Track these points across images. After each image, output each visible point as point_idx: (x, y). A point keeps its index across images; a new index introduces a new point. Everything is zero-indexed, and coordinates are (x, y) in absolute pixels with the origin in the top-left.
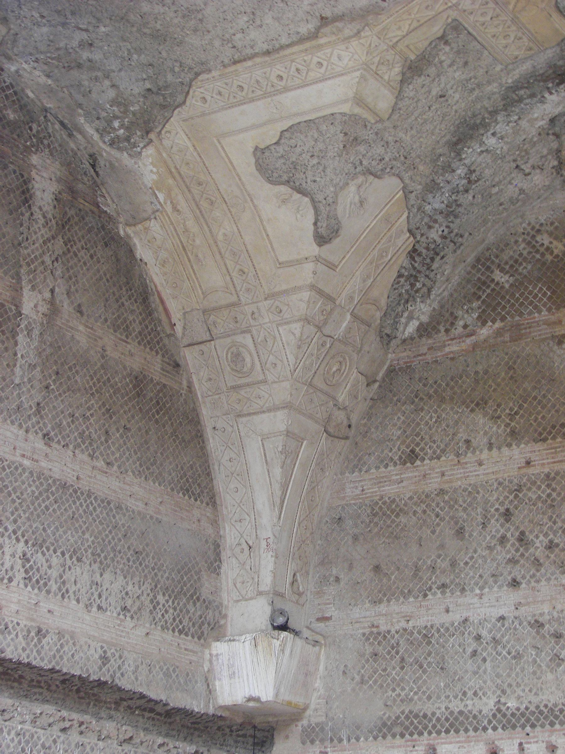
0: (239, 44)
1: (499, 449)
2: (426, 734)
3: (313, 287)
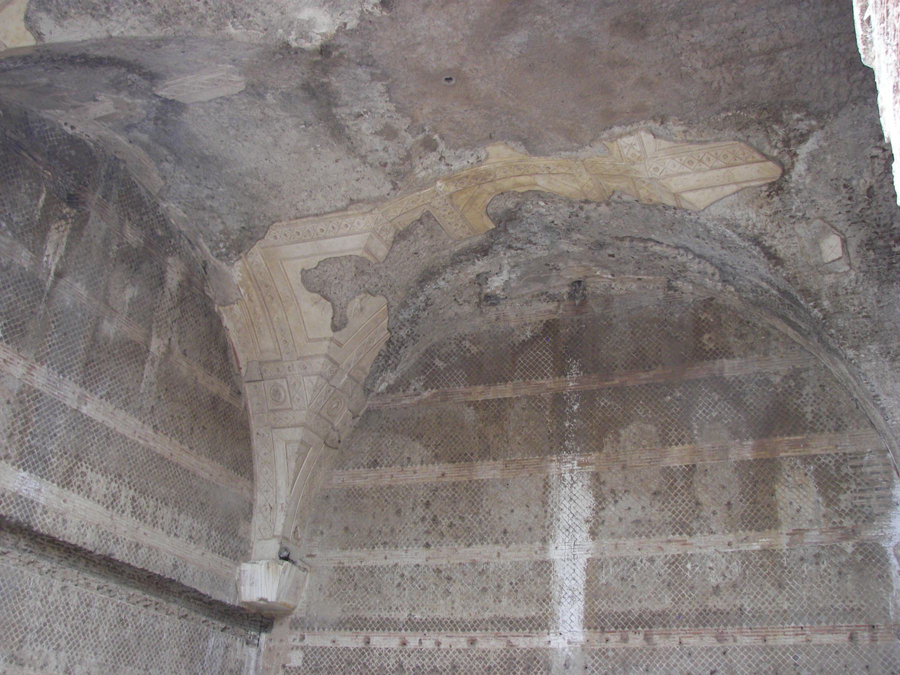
0: (300, 208)
3: (327, 356)
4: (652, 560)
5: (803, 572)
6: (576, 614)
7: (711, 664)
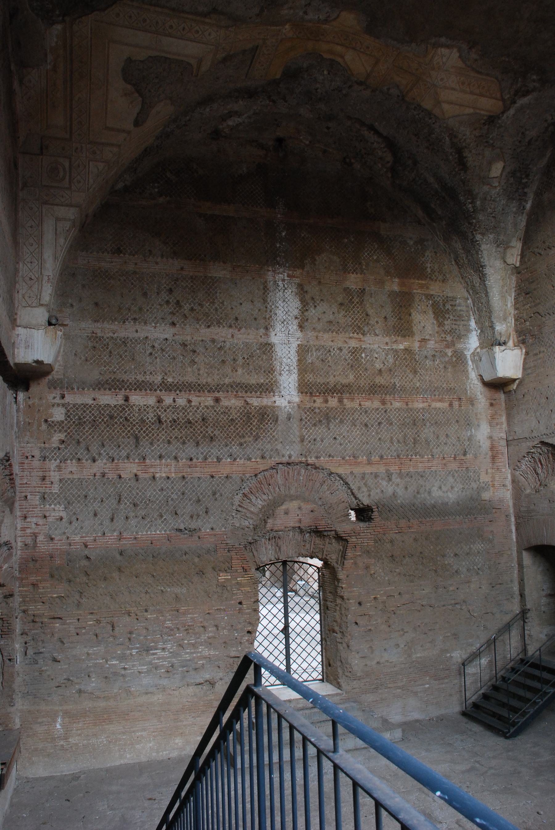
1: (167, 259)
2: (123, 390)
4: (340, 349)
5: (427, 365)
6: (292, 383)
7: (378, 419)
